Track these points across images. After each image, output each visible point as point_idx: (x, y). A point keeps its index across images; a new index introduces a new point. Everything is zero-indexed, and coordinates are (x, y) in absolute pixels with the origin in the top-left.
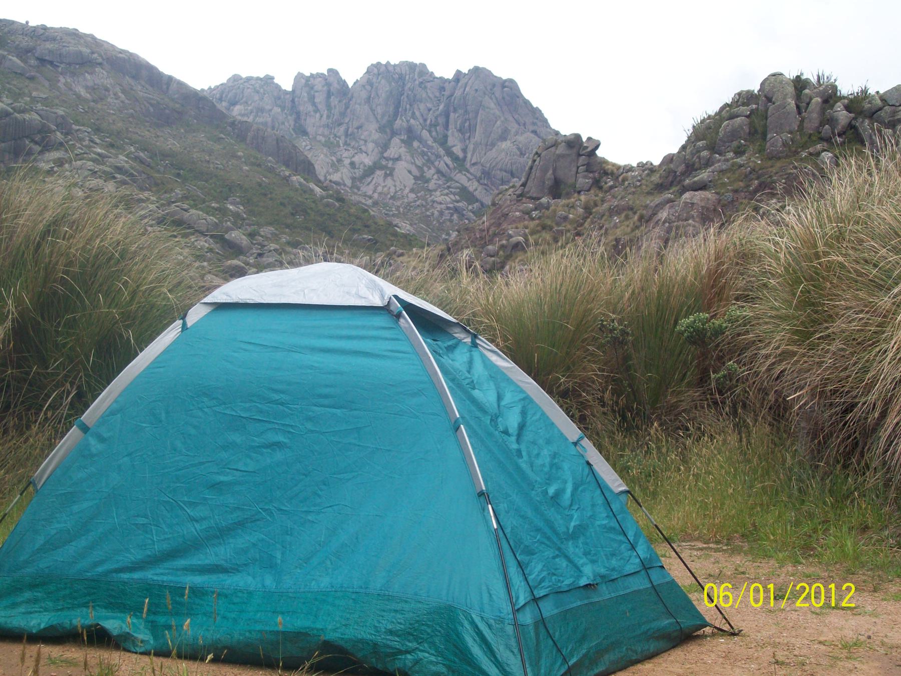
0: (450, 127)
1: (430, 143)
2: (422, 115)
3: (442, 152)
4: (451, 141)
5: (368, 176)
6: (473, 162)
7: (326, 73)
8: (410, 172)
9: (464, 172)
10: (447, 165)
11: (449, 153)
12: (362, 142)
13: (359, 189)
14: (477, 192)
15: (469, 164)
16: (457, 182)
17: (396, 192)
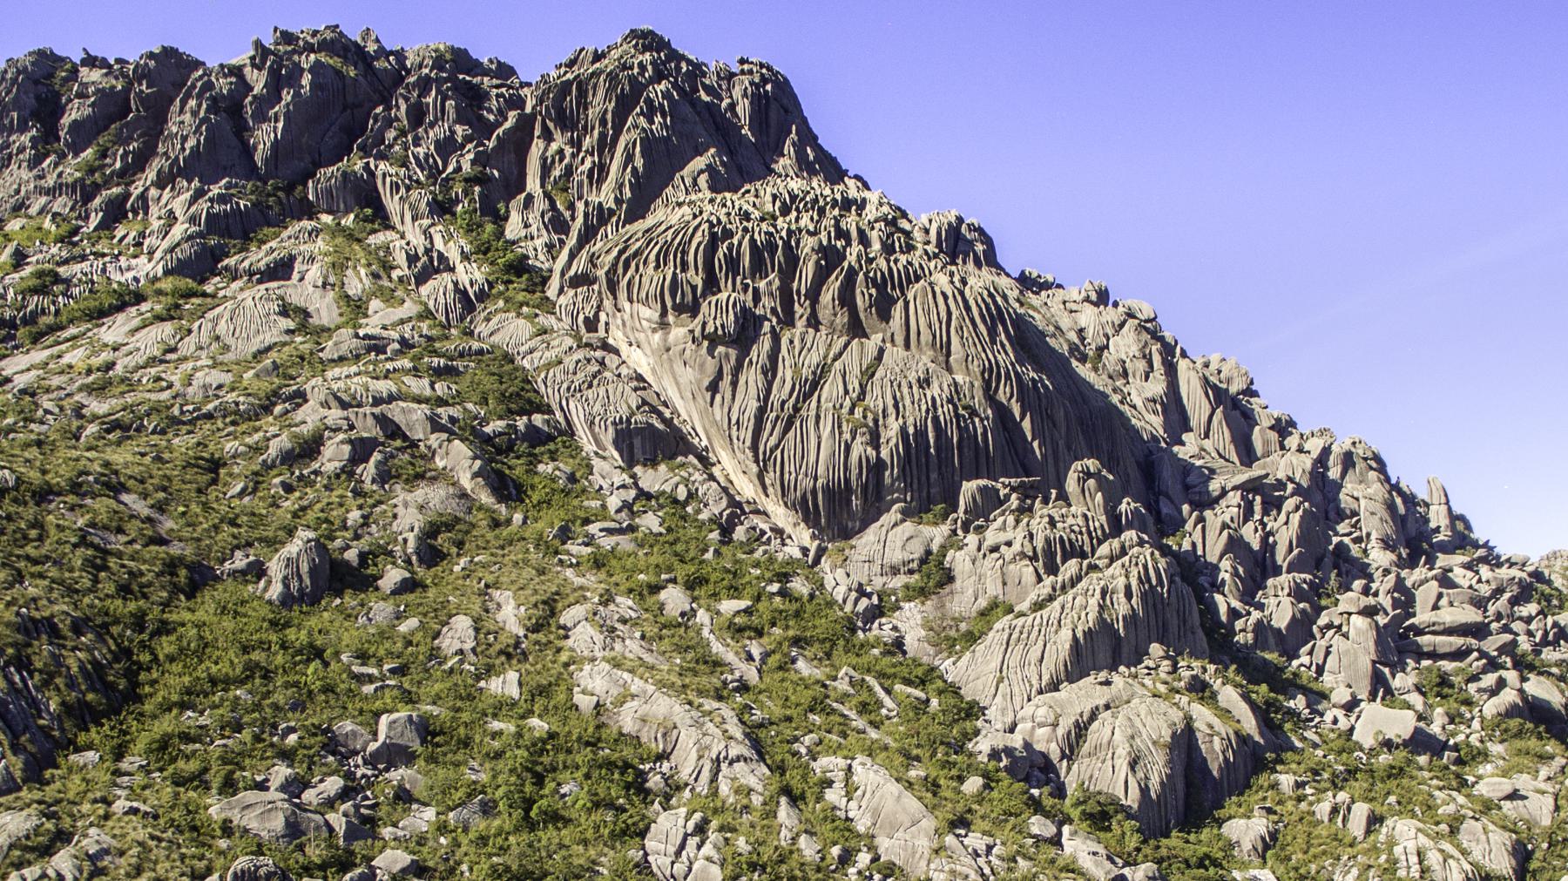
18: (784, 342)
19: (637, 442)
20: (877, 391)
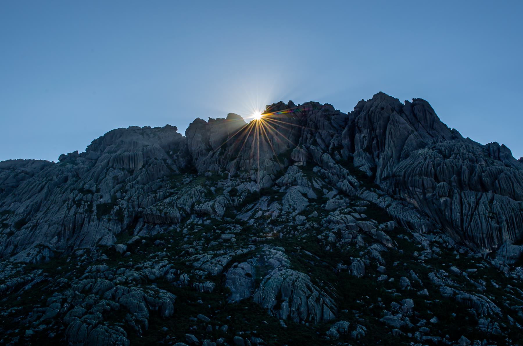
0: (356, 148)
1: (331, 164)
2: (324, 141)
3: (345, 171)
5: (250, 203)
6: (383, 176)
8: (305, 195)
9: (372, 189)
10: (351, 183)
11: (355, 171)
12: (252, 172)
13: (233, 217)
14: (391, 208)
15: (378, 180)
16: (364, 200)
17: (280, 215)
18: (463, 194)
19: (423, 227)
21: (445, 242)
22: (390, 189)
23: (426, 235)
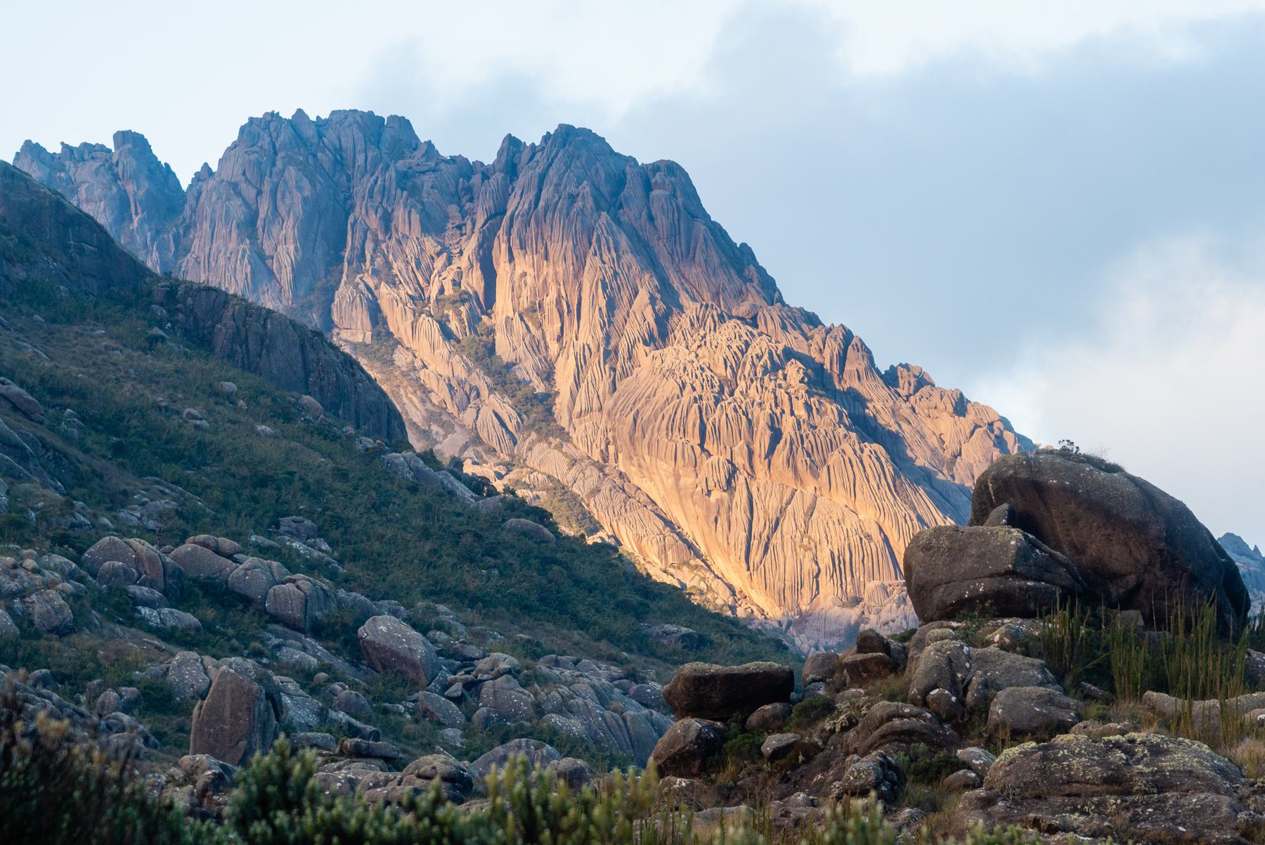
3: (481, 381)
4: (504, 350)
6: (577, 409)
7: (110, 145)
10: (497, 415)
19: (669, 553)
20: (815, 526)
21: (709, 588)
22: (594, 446)
23: (671, 570)
